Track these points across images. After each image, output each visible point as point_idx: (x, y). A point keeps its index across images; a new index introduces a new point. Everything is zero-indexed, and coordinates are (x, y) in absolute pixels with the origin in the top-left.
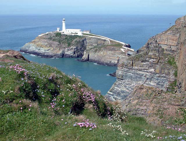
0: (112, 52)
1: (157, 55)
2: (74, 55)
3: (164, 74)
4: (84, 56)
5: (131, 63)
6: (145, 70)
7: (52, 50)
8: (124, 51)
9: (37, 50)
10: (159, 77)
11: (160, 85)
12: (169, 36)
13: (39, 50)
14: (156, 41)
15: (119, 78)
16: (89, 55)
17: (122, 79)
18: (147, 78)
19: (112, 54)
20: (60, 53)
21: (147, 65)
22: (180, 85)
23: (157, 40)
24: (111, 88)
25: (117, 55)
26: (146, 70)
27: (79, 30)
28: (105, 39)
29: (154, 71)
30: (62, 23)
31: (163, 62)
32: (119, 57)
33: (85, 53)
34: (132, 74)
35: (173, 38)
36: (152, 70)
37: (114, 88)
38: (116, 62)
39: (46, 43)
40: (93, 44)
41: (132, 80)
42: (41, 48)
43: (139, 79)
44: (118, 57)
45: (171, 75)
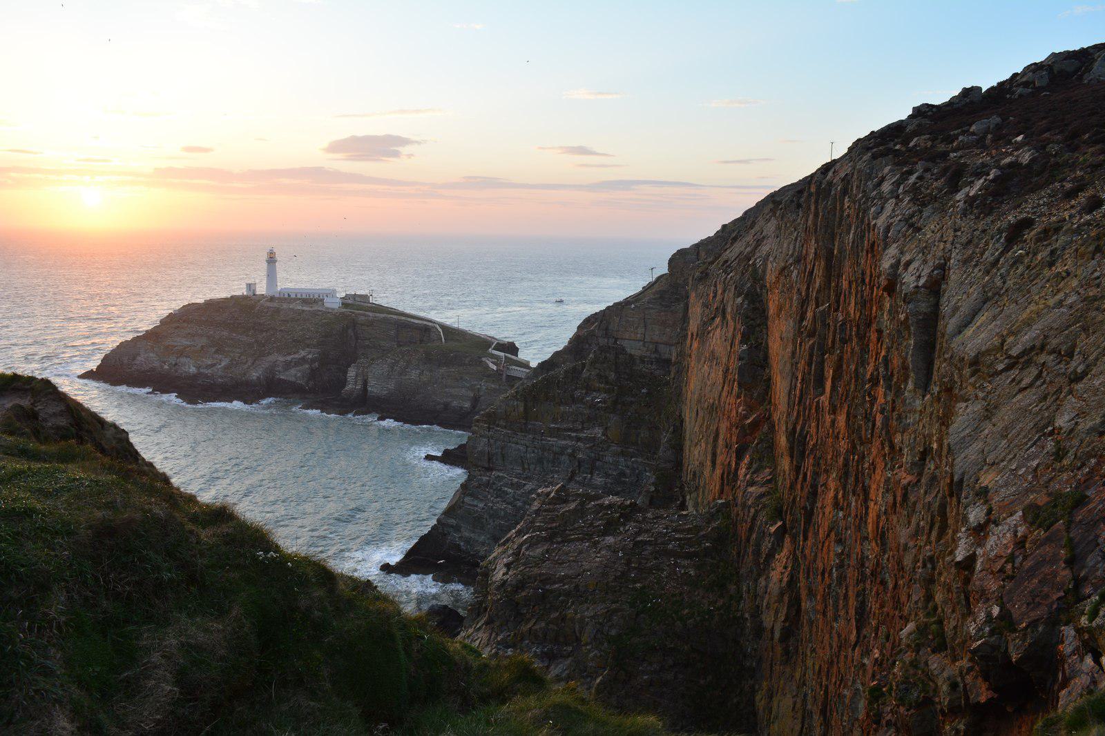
1: (612, 376)
2: (311, 383)
4: (349, 387)
5: (522, 409)
7: (226, 368)
8: (495, 368)
9: (166, 367)
10: (623, 454)
11: (625, 482)
12: (652, 311)
13: (176, 364)
14: (607, 329)
16: (365, 383)
17: (490, 469)
18: (579, 462)
20: (255, 378)
22: (694, 479)
23: (611, 327)
26: (576, 431)
28: (425, 323)
29: (603, 435)
31: (632, 403)
32: (479, 390)
33: (351, 373)
35: (663, 318)
36: (598, 432)
37: (463, 502)
38: (467, 405)
39: (204, 341)
40: (382, 343)
41: (524, 469)
42: (183, 360)
43: (550, 464)
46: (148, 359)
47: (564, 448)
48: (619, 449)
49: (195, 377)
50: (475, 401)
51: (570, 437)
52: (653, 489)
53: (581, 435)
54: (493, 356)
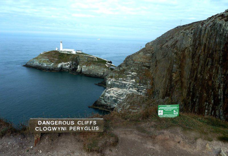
0: (99, 67)
1: (137, 69)
3: (142, 83)
6: (129, 81)
10: (139, 85)
15: (109, 86)
16: (81, 69)
19: (99, 68)
21: (129, 76)
24: (102, 94)
25: (102, 69)
27: (73, 50)
30: (60, 44)
33: (78, 67)
34: (118, 84)
36: (134, 80)
38: (102, 74)
42: (44, 63)
44: (103, 70)
45: (148, 84)
46: (36, 63)
47: (127, 84)
48: (139, 84)
49: (46, 67)
50: (104, 73)
51: (128, 82)
52: (146, 93)
53: (130, 81)
54: (107, 64)
